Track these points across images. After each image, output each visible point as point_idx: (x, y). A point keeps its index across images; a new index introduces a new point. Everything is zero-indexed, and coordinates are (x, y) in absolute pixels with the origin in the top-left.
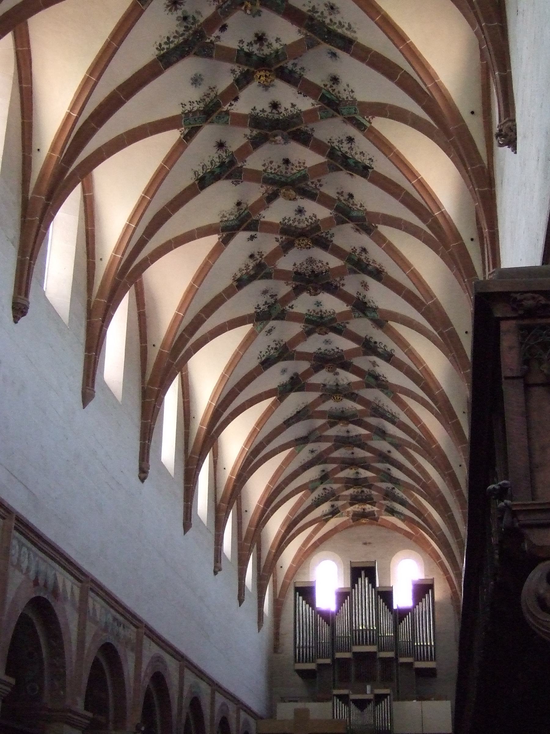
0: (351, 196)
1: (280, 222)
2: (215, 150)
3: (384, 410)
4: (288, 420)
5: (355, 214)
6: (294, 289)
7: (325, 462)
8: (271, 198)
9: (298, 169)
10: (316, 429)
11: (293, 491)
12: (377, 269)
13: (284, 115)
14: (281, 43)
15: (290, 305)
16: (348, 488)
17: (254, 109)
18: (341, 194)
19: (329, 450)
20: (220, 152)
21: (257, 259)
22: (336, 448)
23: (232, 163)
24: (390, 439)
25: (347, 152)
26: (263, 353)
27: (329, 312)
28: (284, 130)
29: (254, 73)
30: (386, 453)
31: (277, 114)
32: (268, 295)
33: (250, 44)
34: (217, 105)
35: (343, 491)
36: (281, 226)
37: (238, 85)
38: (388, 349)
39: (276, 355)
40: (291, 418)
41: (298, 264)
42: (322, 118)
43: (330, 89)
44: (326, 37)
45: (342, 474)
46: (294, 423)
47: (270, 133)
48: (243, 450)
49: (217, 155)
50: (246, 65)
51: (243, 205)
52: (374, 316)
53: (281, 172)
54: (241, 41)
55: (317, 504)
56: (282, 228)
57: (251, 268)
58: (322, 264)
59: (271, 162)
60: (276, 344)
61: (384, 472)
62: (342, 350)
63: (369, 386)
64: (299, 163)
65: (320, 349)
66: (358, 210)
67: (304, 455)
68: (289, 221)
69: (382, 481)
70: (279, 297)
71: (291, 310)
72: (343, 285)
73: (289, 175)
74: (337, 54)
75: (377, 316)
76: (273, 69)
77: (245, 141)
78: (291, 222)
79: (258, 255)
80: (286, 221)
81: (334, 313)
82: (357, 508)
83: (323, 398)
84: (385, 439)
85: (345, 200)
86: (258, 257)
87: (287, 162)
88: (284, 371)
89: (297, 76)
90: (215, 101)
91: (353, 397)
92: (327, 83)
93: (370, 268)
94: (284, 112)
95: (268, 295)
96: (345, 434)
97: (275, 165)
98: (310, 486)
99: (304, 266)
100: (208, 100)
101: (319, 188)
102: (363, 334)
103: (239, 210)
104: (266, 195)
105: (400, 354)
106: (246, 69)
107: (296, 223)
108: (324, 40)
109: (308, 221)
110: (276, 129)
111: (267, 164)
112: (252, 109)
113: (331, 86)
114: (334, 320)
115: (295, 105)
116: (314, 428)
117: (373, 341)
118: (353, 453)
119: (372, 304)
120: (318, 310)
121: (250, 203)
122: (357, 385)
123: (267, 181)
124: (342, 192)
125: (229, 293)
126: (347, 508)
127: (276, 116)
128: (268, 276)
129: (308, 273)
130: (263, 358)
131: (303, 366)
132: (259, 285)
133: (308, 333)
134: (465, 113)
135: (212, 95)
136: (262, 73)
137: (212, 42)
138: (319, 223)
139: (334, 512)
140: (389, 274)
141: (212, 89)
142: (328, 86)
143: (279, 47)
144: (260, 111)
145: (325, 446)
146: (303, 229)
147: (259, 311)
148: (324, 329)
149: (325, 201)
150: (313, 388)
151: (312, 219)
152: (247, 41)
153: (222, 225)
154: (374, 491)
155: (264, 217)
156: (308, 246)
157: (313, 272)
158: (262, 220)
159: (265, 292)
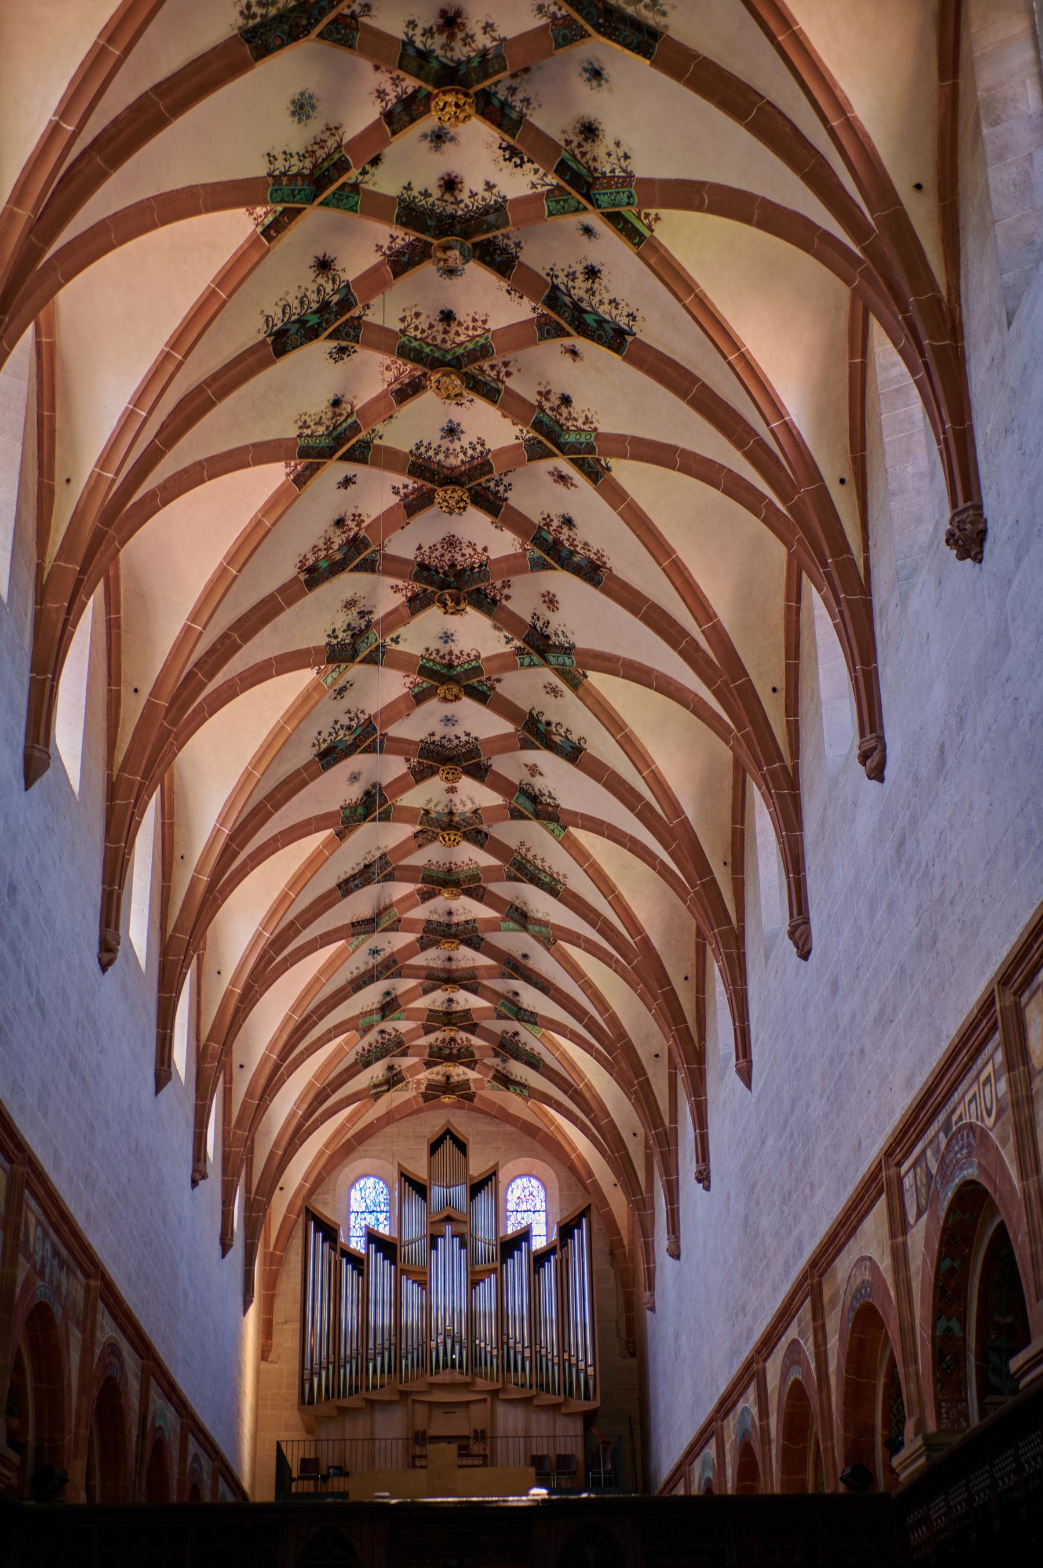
0: (566, 400)
1: (411, 452)
2: (311, 274)
3: (537, 867)
4: (346, 881)
5: (571, 438)
6: (410, 600)
7: (398, 975)
9: (471, 333)
10: (391, 906)
11: (329, 1031)
12: (591, 562)
13: (467, 206)
14: (495, 34)
15: (394, 635)
16: (428, 1030)
17: (408, 187)
18: (546, 395)
19: (409, 951)
20: (321, 280)
21: (350, 530)
22: (424, 945)
24: (537, 928)
25: (581, 300)
26: (325, 735)
27: (468, 655)
28: (466, 235)
29: (429, 97)
30: (520, 958)
31: (452, 203)
32: (355, 611)
33: (428, 32)
34: (342, 166)
35: (419, 1037)
36: (412, 459)
37: (390, 123)
38: (574, 737)
39: (350, 739)
40: (353, 877)
41: (426, 548)
42: (551, 214)
43: (577, 152)
44: (601, 21)
45: (422, 1003)
46: (357, 887)
47: (435, 242)
48: (258, 936)
49: (314, 287)
50: (417, 76)
51: (344, 405)
52: (564, 665)
53: (434, 338)
54: (412, 24)
55: (365, 1062)
56: (413, 464)
57: (335, 546)
58: (474, 549)
59: (417, 315)
60: (351, 719)
61: (506, 998)
62: (476, 739)
63: (517, 815)
64: (474, 320)
65: (432, 734)
66: (580, 430)
67: (359, 961)
68: (427, 451)
69: (500, 1017)
70: (378, 615)
71: (394, 646)
72: (508, 598)
73: (448, 345)
74: (604, 73)
76: (471, 92)
77: (376, 258)
78: (431, 453)
79: (353, 520)
80: (422, 450)
81: (477, 657)
83: (421, 839)
84: (526, 930)
85: (552, 409)
86: (352, 525)
87: (447, 317)
88: (354, 778)
89: (514, 116)
90: (336, 156)
91: (479, 838)
92: (572, 137)
93: (577, 559)
94: (467, 201)
95: (355, 611)
96: (443, 919)
97: (423, 323)
98: (362, 1022)
99: (438, 553)
100: (321, 154)
101: (505, 379)
103: (335, 415)
104: (396, 386)
106: (410, 90)
107: (441, 457)
108: (597, 27)
109: (465, 453)
110: (447, 235)
111: (409, 318)
112: (404, 188)
113: (580, 146)
114: (477, 671)
115: (494, 186)
116: (388, 902)
117: (543, 719)
118: (450, 959)
119: (562, 638)
120: (444, 649)
121: (359, 404)
122: (495, 814)
123: (405, 352)
124: (548, 392)
126: (418, 1073)
127: (450, 209)
128: (368, 566)
129: (442, 567)
130: (324, 746)
133: (420, 698)
135: (331, 143)
136: (450, 98)
137: (353, 16)
138: (489, 456)
139: (393, 1080)
140: (615, 572)
142: (574, 145)
143: (489, 44)
144: (420, 193)
145: (402, 939)
146: (452, 469)
147: (334, 642)
148: (455, 689)
150: (407, 815)
151: (474, 449)
152: (422, 25)
153: (302, 442)
154: (479, 1037)
155: (381, 437)
156: (462, 505)
157: (453, 566)
158: (377, 442)
159: (350, 604)
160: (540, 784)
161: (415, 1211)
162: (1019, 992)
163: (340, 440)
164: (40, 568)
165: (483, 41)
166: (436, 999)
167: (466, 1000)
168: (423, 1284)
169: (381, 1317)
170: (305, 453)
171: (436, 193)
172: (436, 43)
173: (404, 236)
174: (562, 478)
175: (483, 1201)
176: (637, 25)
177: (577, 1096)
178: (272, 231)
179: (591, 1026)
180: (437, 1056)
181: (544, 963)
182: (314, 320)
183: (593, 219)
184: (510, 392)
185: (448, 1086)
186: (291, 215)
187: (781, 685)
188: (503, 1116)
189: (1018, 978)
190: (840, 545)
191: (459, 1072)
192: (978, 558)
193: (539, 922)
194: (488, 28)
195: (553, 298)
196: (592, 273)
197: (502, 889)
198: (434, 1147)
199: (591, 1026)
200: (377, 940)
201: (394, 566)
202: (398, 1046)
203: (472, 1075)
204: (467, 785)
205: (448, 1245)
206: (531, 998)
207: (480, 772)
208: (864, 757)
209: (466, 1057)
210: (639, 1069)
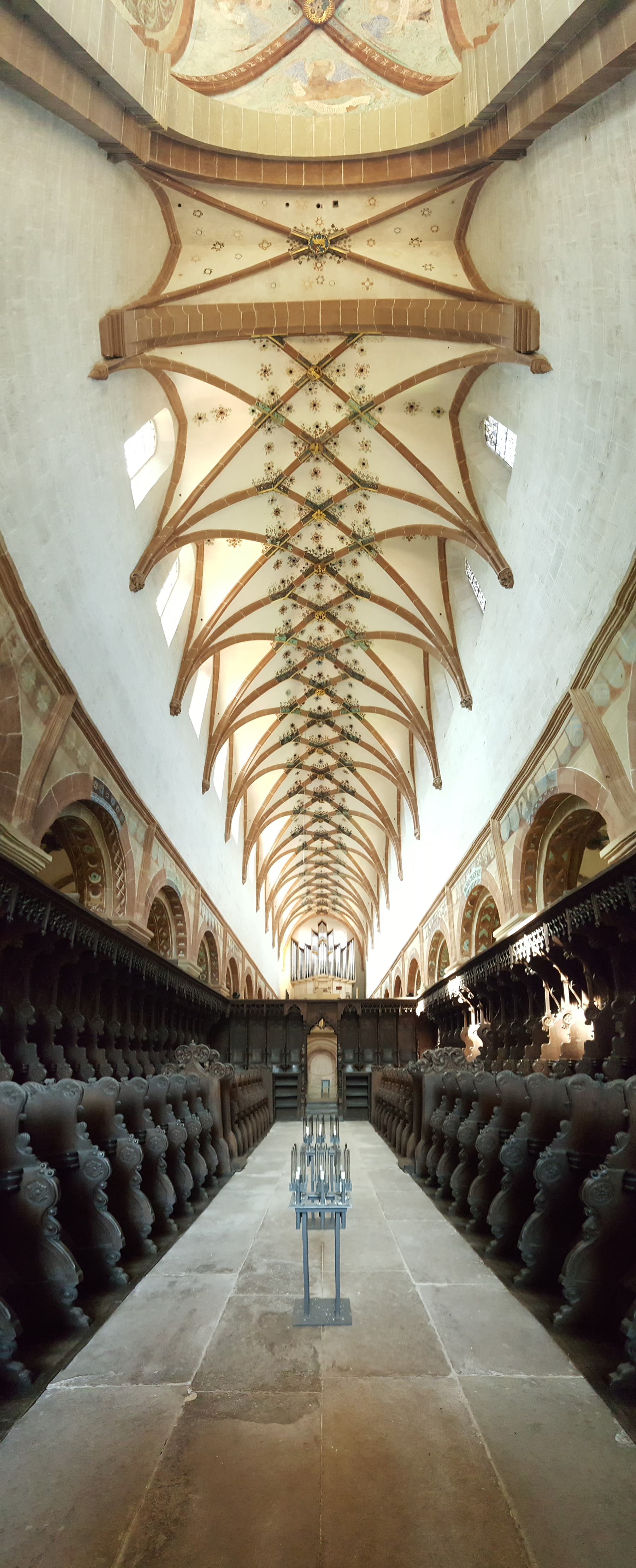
0: (346, 754)
5: (347, 762)
8: (311, 753)
16: (317, 898)
18: (342, 753)
19: (312, 880)
22: (316, 878)
23: (297, 734)
33: (315, 677)
34: (296, 705)
55: (303, 906)
63: (337, 848)
67: (302, 882)
69: (333, 895)
75: (347, 813)
77: (304, 724)
82: (320, 908)
87: (320, 736)
88: (300, 840)
102: (338, 824)
105: (355, 832)
114: (327, 816)
122: (331, 849)
123: (310, 744)
125: (285, 799)
128: (302, 793)
131: (309, 838)
132: (298, 796)
133: (314, 822)
134: (419, 708)
139: (310, 909)
141: (294, 697)
149: (334, 756)
150: (312, 849)
159: (298, 801)
160: (343, 841)
161: (315, 937)
162: (451, 887)
163: (296, 764)
164: (229, 794)
165: (327, 679)
166: (319, 891)
167: (325, 891)
168: (317, 955)
169: (308, 962)
170: (288, 767)
171: (317, 710)
172: (317, 679)
173: (310, 719)
174: (346, 772)
175: (330, 936)
176: (359, 675)
177: (351, 913)
178: (281, 718)
179: (354, 897)
180: (319, 904)
181: (342, 882)
182: (290, 737)
183: (351, 715)
184: (334, 753)
185: (322, 911)
186: (285, 715)
187: (396, 818)
188: (335, 917)
189: (450, 884)
190: (409, 786)
191: (324, 908)
192: (440, 789)
193: (342, 874)
194: (328, 676)
195: (343, 732)
196: (351, 726)
197: (333, 866)
198: (319, 925)
199: (354, 897)
200: (305, 877)
201: (308, 792)
202: (311, 902)
203: (327, 908)
204: (325, 841)
205: (322, 945)
206: (340, 891)
207: (328, 839)
208: (415, 834)
209: (326, 904)
210: (364, 907)
